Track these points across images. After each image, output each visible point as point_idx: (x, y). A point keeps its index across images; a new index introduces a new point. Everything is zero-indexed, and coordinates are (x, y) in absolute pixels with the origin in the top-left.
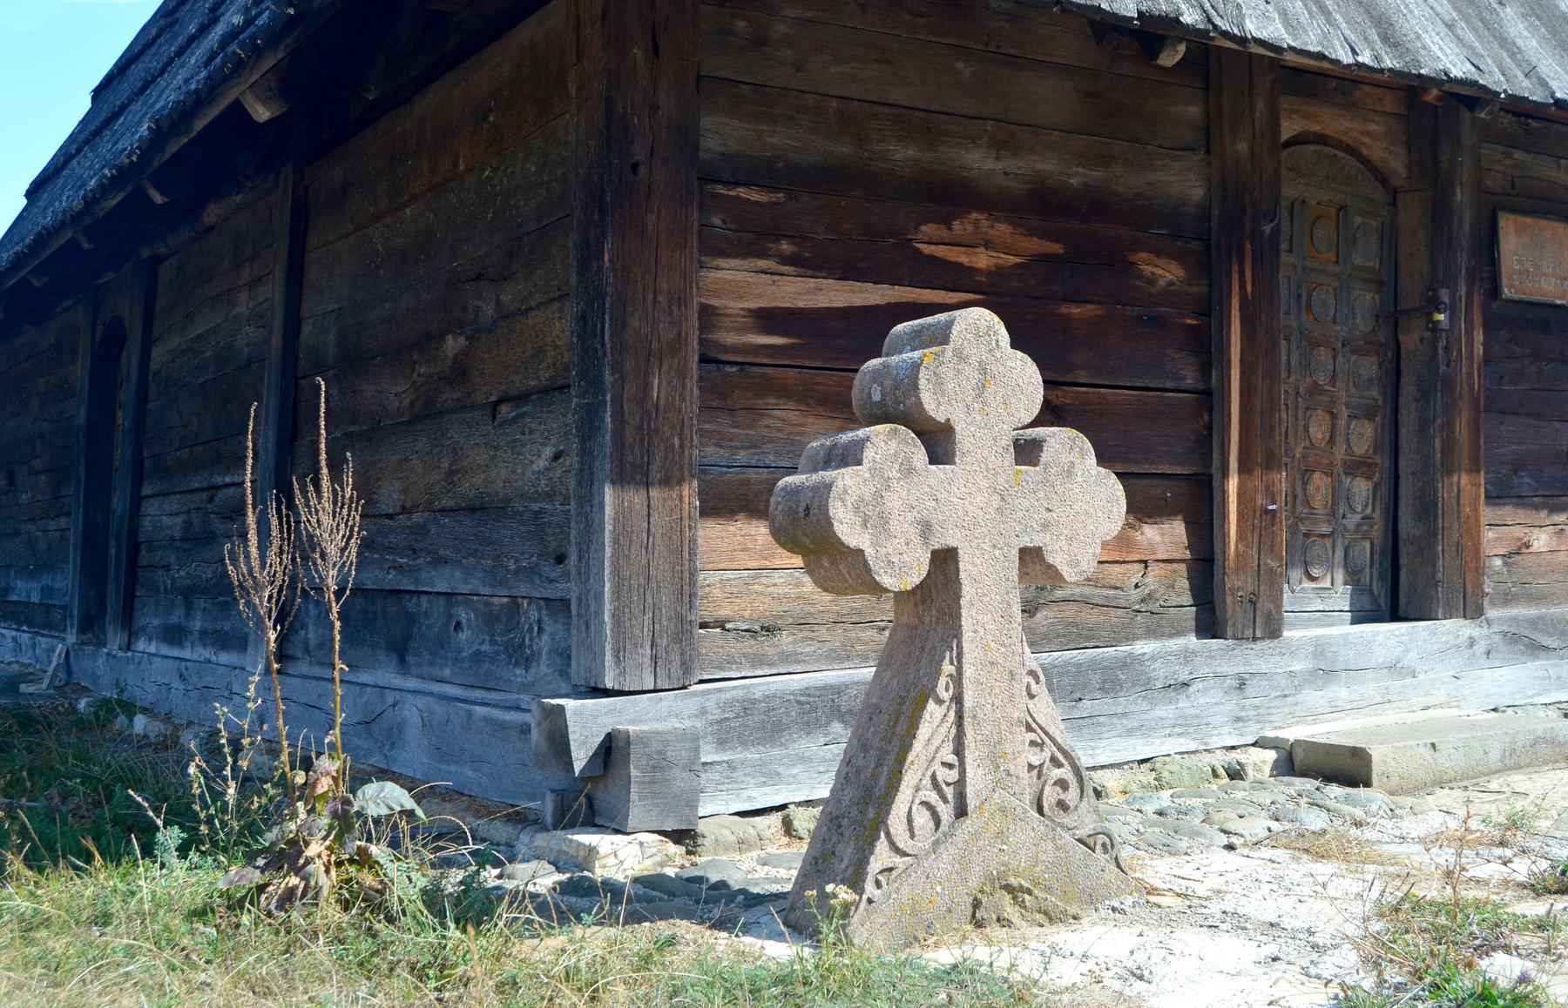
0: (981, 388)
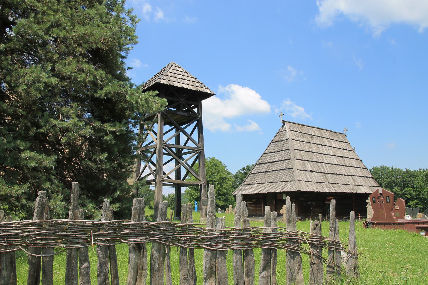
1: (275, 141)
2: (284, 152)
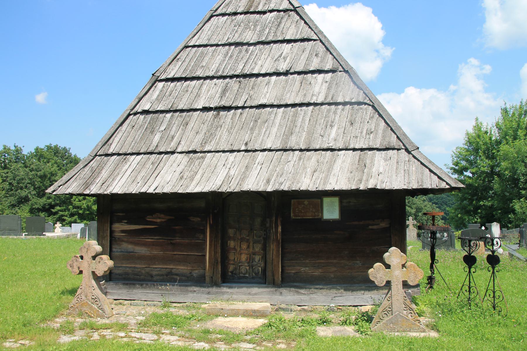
0: (87, 252)
1: (229, 11)
2: (290, 45)
